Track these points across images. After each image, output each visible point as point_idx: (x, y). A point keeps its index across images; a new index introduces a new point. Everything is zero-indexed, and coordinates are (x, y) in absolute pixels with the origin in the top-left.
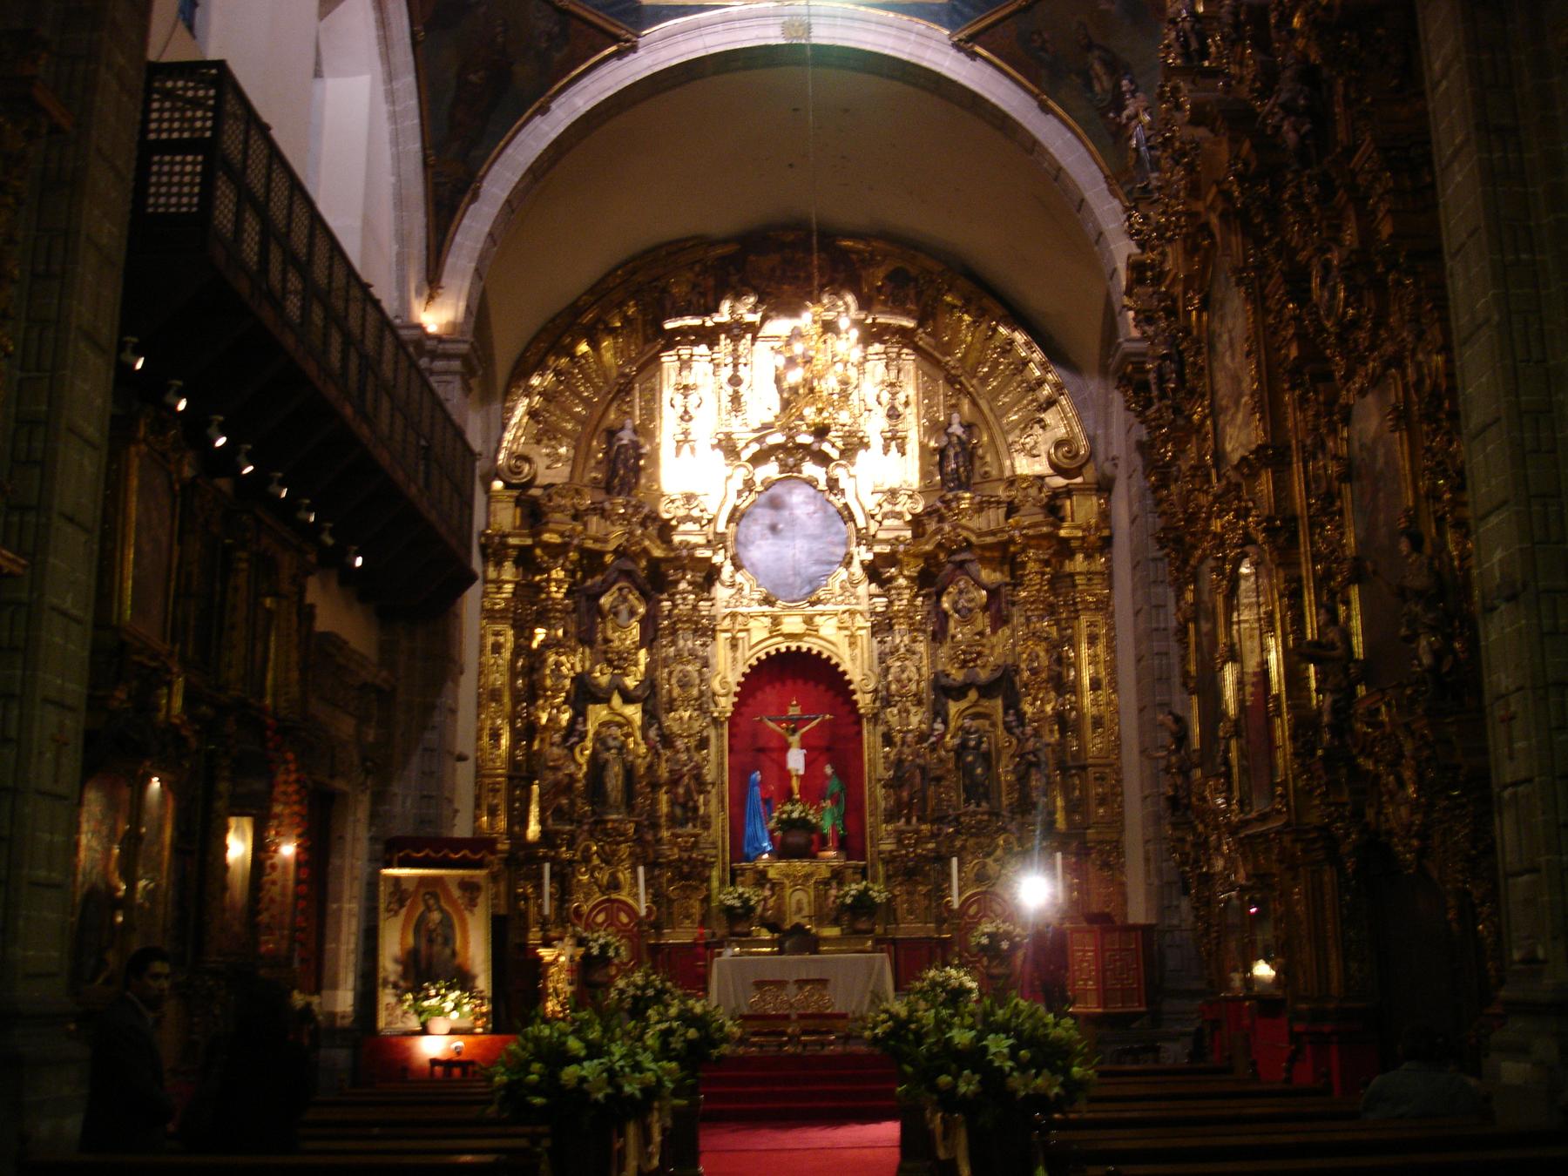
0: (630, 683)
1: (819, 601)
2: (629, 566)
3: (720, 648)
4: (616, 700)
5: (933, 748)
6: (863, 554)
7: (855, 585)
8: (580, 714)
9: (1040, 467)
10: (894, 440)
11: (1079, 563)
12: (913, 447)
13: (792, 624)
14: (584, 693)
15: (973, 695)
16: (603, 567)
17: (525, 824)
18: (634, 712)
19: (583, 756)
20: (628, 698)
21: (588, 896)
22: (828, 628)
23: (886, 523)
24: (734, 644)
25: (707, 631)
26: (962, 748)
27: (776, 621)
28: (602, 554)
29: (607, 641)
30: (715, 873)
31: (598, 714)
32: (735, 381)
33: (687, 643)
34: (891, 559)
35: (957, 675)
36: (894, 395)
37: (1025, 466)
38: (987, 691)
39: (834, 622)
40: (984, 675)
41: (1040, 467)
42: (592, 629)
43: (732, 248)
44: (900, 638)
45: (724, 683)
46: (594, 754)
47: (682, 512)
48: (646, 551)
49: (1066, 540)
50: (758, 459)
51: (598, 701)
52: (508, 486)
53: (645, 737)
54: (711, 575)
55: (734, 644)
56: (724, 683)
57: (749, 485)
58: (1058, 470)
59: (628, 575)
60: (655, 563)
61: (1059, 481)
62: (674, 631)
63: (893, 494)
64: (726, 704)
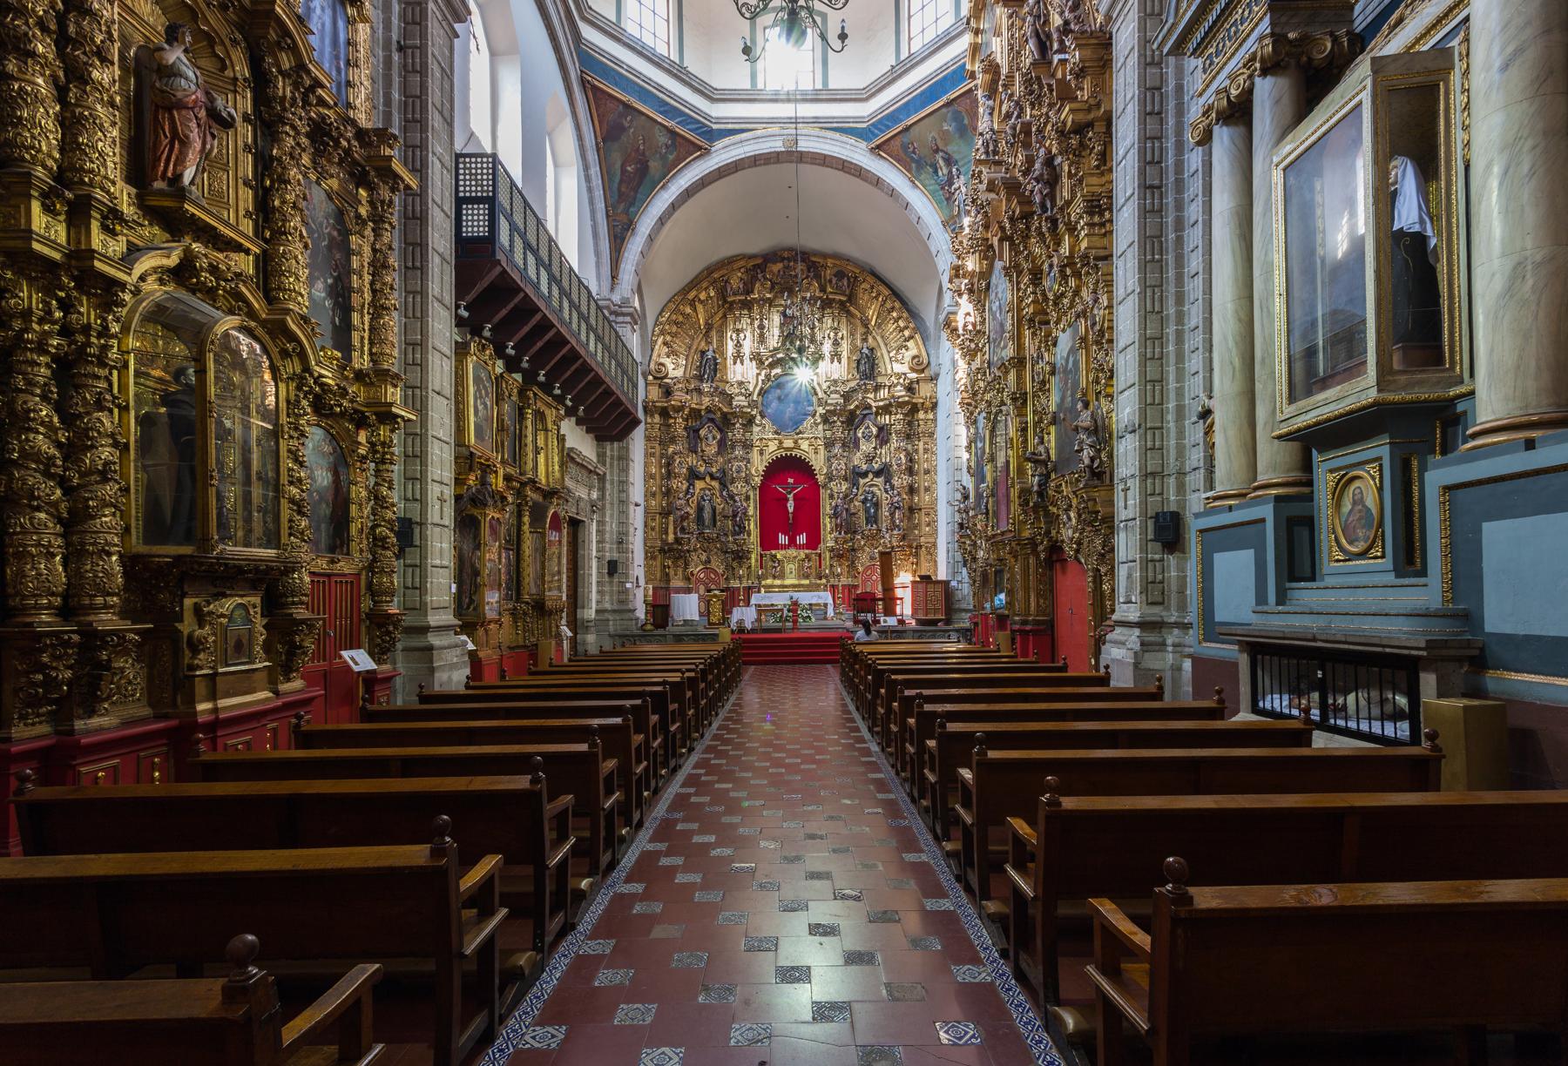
0: (714, 470)
1: (800, 432)
2: (712, 416)
3: (755, 454)
4: (708, 479)
5: (852, 500)
6: (821, 410)
7: (817, 425)
8: (692, 484)
9: (904, 368)
10: (836, 356)
11: (921, 415)
12: (844, 361)
13: (788, 443)
14: (693, 475)
15: (871, 476)
16: (701, 417)
17: (667, 533)
18: (715, 484)
19: (694, 501)
20: (713, 477)
21: (696, 567)
22: (805, 445)
23: (833, 396)
24: (761, 453)
25: (748, 446)
26: (864, 501)
27: (781, 443)
28: (700, 411)
29: (703, 451)
30: (753, 556)
31: (699, 485)
32: (761, 327)
33: (739, 452)
34: (833, 413)
35: (864, 467)
36: (836, 334)
37: (898, 368)
38: (878, 474)
39: (807, 442)
40: (876, 466)
41: (904, 368)
42: (696, 446)
43: (759, 261)
44: (837, 450)
45: (757, 470)
46: (699, 503)
47: (737, 391)
48: (720, 409)
49: (916, 404)
50: (772, 366)
51: (699, 478)
52: (655, 378)
53: (721, 495)
54: (750, 421)
55: (761, 453)
56: (757, 470)
57: (768, 377)
58: (913, 370)
59: (712, 420)
60: (725, 415)
61: (913, 376)
62: (733, 448)
63: (835, 381)
64: (758, 480)
